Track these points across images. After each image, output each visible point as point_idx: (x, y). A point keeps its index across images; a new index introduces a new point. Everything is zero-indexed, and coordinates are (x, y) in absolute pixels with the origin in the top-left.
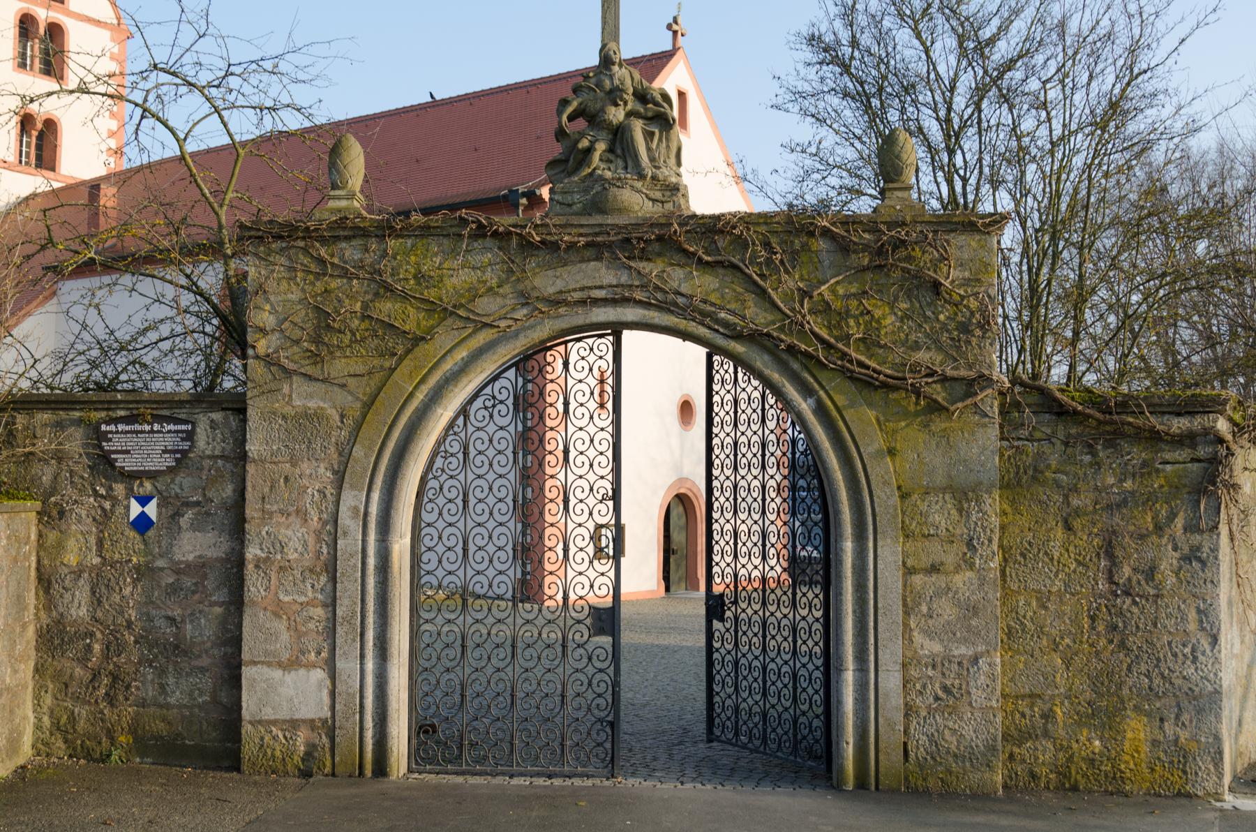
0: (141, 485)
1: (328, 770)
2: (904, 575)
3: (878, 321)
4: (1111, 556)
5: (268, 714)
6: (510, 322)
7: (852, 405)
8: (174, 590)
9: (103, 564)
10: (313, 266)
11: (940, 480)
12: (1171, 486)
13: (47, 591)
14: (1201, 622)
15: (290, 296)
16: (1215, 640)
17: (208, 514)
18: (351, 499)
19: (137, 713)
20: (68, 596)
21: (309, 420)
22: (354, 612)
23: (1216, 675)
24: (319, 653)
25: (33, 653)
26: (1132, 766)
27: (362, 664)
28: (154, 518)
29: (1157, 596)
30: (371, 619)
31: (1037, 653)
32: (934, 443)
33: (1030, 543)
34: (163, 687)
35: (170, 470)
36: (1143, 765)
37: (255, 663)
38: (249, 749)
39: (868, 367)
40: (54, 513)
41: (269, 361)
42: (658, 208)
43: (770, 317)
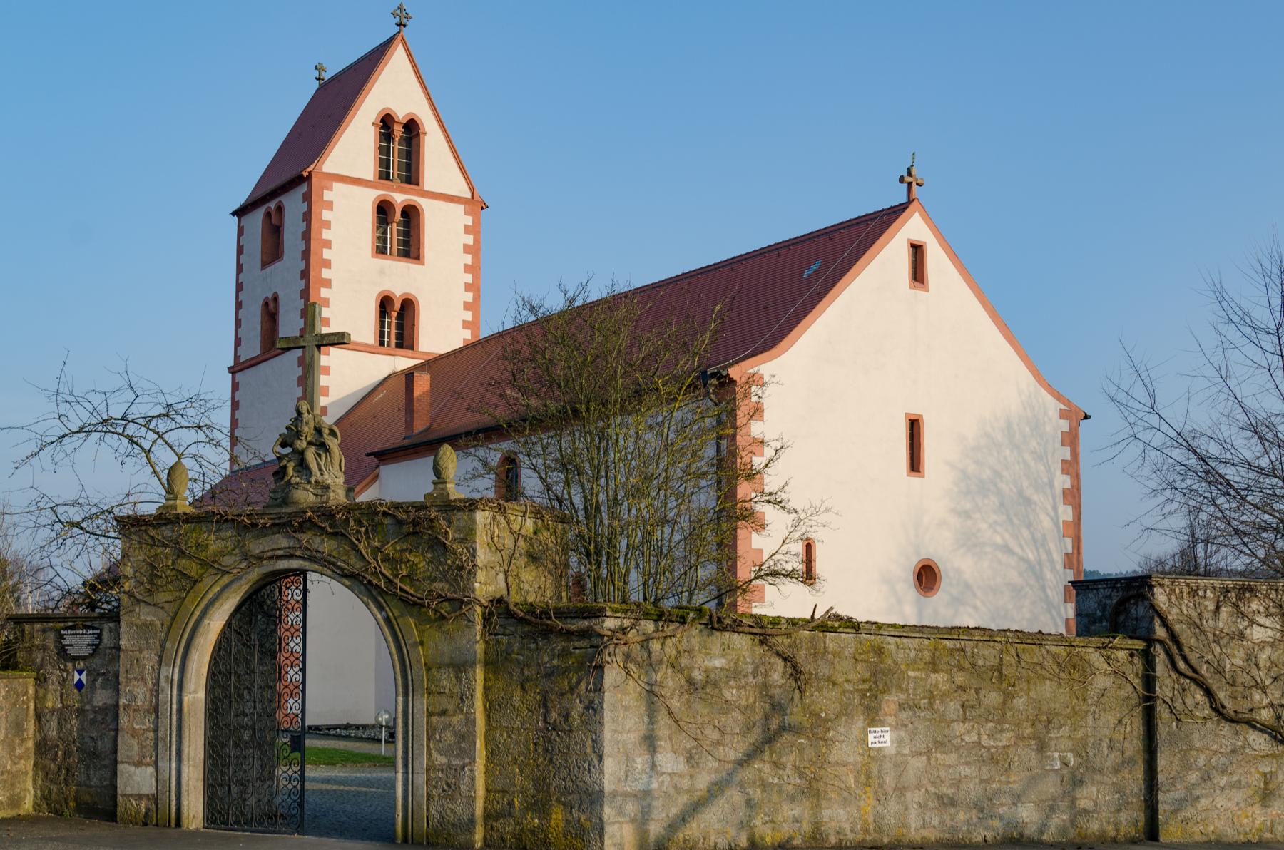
0: (79, 664)
1: (154, 822)
2: (427, 716)
3: (416, 565)
4: (545, 706)
5: (129, 791)
6: (239, 570)
7: (402, 615)
8: (93, 722)
9: (63, 707)
10: (150, 540)
11: (447, 659)
12: (578, 663)
13: (39, 721)
14: (594, 747)
15: (140, 558)
16: (601, 758)
17: (108, 679)
18: (165, 671)
19: (77, 790)
20: (48, 725)
21: (146, 628)
22: (166, 735)
23: (601, 780)
24: (151, 758)
25: (32, 756)
26: (554, 835)
27: (170, 764)
28: (85, 682)
29: (570, 731)
30: (174, 739)
31: (506, 765)
32: (443, 637)
33: (503, 698)
35: (91, 655)
36: (561, 835)
37: (123, 762)
38: (120, 810)
39: (407, 593)
40: (42, 679)
41: (130, 594)
42: (319, 499)
43: (362, 564)
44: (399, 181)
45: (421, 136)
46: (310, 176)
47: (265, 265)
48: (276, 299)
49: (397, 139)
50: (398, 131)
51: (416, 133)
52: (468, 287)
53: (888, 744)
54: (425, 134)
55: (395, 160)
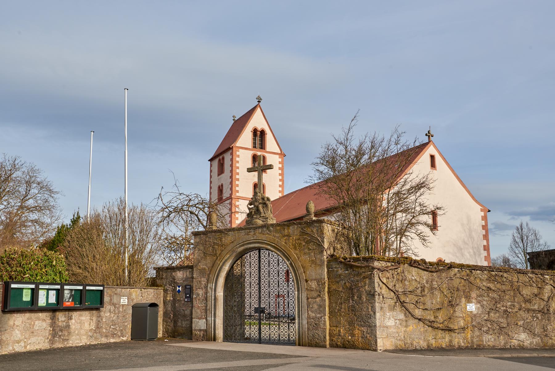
5: (197, 328)
8: (183, 304)
13: (165, 305)
16: (375, 313)
28: (181, 290)
29: (362, 303)
30: (213, 310)
34: (182, 323)
37: (194, 318)
47: (219, 175)
48: (222, 185)
50: (259, 133)
53: (474, 310)
55: (258, 142)
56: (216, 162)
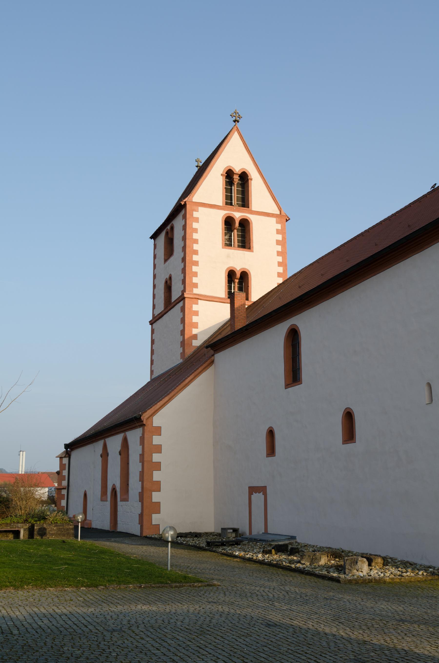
44: (238, 206)
45: (249, 181)
46: (185, 204)
47: (166, 260)
48: (170, 278)
49: (236, 183)
50: (236, 178)
51: (247, 180)
52: (280, 264)
54: (251, 179)
56: (162, 238)
